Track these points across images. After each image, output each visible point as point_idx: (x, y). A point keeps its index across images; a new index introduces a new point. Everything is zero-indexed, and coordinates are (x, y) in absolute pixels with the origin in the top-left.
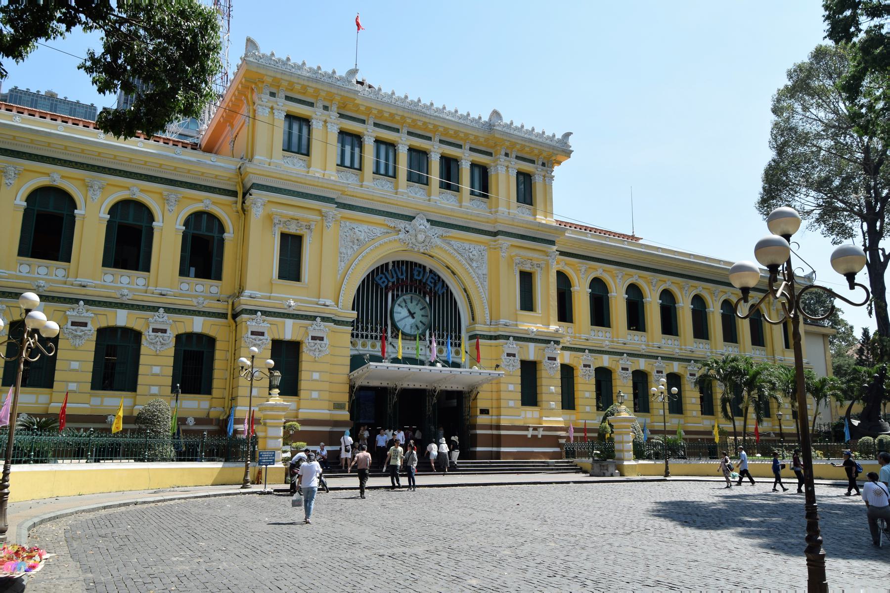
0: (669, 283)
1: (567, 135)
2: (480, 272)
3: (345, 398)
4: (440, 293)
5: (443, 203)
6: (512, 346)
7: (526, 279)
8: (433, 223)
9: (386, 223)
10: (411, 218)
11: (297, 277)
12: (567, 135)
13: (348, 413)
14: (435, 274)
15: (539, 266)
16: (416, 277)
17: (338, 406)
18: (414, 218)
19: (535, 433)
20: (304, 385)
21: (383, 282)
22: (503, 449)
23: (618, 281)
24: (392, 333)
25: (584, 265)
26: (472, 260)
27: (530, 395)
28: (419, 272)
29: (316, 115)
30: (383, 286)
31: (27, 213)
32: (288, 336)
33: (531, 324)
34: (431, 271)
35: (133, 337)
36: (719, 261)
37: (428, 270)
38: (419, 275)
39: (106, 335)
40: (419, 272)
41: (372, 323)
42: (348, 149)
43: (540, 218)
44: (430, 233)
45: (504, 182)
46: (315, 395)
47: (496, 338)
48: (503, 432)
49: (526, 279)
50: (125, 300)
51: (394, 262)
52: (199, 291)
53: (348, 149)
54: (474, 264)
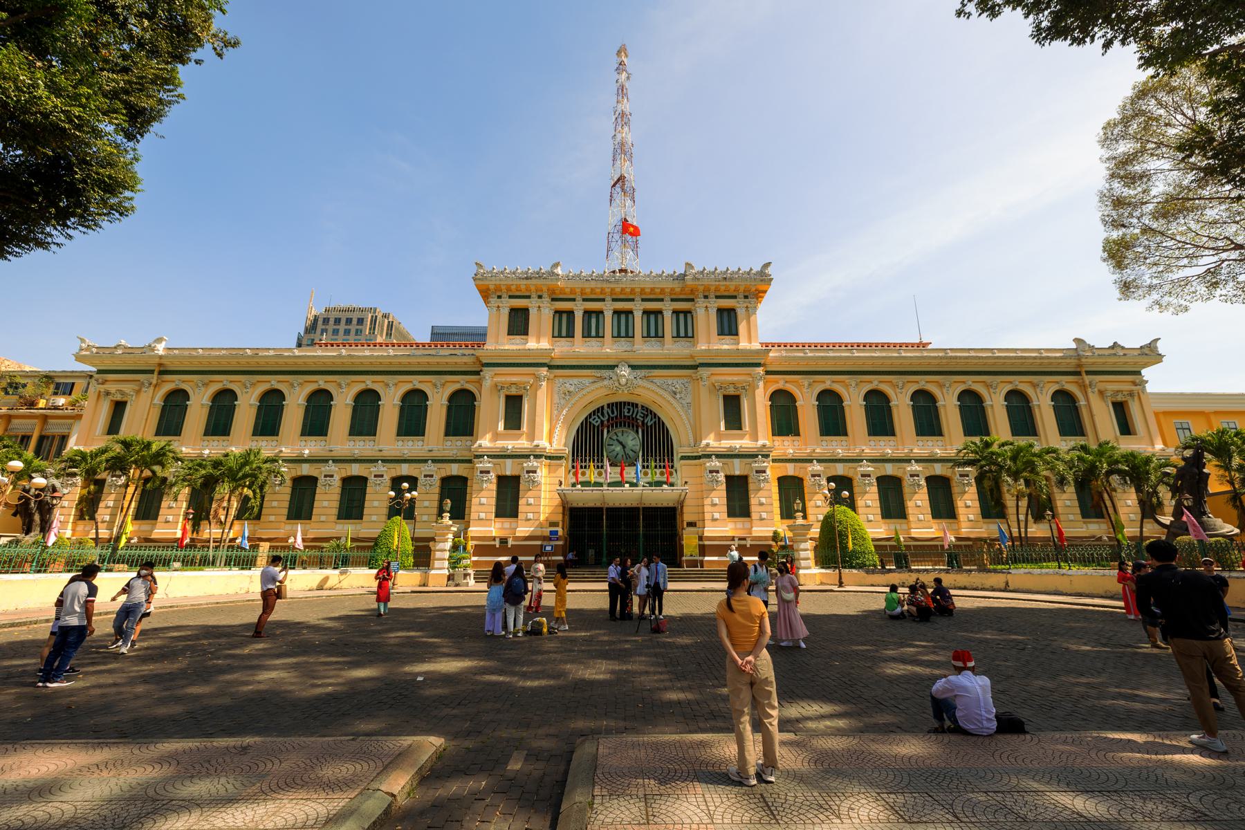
0: (876, 383)
1: (767, 265)
5: (646, 350)
6: (715, 463)
10: (612, 367)
11: (518, 426)
12: (767, 265)
15: (743, 388)
19: (743, 542)
20: (521, 509)
22: (707, 558)
23: (851, 390)
25: (805, 380)
27: (739, 504)
29: (531, 304)
31: (402, 409)
35: (363, 481)
36: (1015, 350)
39: (347, 481)
43: (744, 344)
45: (705, 318)
47: (699, 457)
48: (706, 543)
50: (406, 457)
52: (455, 446)
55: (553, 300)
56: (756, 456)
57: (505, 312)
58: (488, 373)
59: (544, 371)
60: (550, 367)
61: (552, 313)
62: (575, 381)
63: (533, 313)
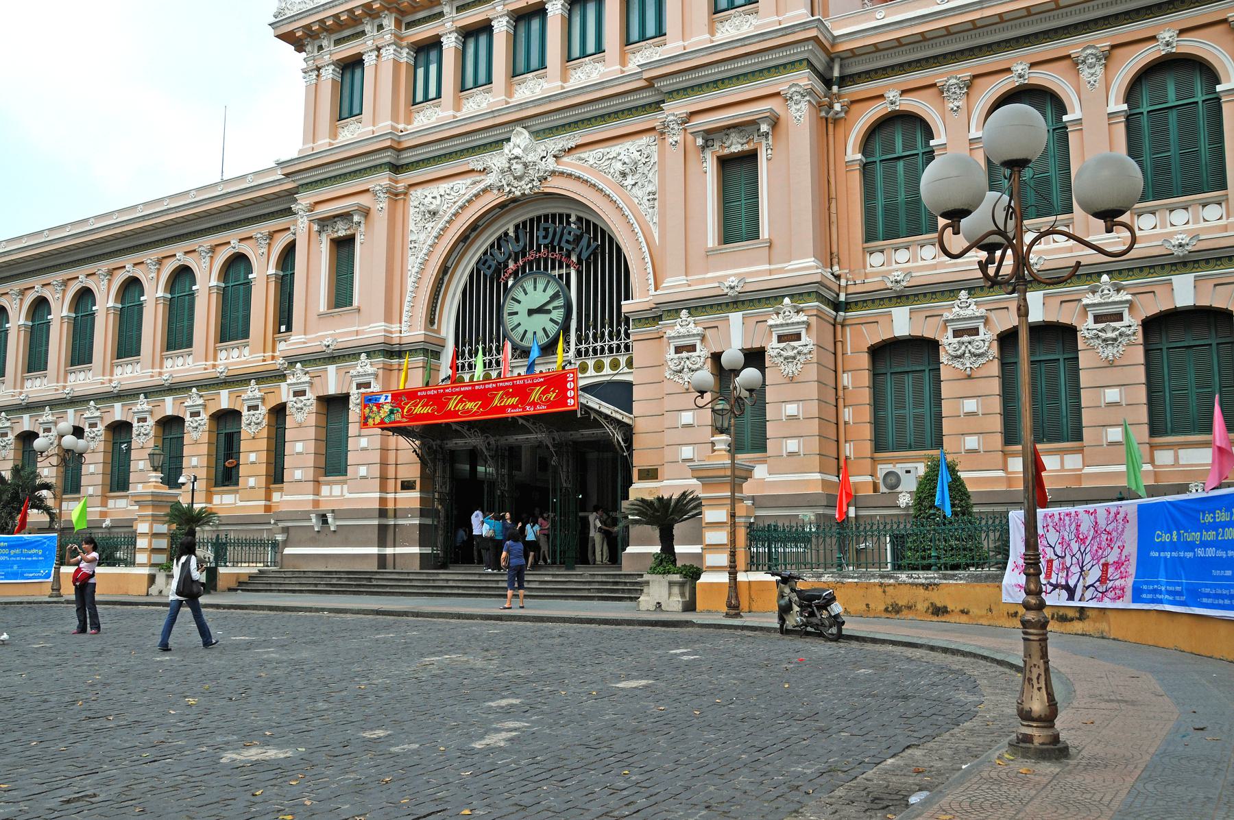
2: (640, 194)
3: (412, 471)
4: (584, 256)
7: (738, 170)
8: (538, 134)
9: (471, 167)
13: (415, 495)
14: (588, 222)
16: (541, 241)
17: (407, 486)
18: (508, 140)
20: (352, 458)
21: (489, 267)
24: (514, 349)
26: (624, 175)
28: (546, 229)
30: (489, 273)
32: (332, 390)
33: (743, 270)
34: (580, 219)
37: (573, 219)
38: (545, 237)
40: (546, 229)
41: (484, 343)
42: (433, 68)
44: (530, 158)
46: (363, 471)
49: (738, 170)
51: (517, 227)
53: (433, 68)
54: (630, 181)
55: (409, 25)
56: (778, 299)
57: (328, 73)
58: (304, 200)
59: (382, 180)
60: (396, 168)
61: (405, 56)
62: (444, 187)
63: (369, 60)
